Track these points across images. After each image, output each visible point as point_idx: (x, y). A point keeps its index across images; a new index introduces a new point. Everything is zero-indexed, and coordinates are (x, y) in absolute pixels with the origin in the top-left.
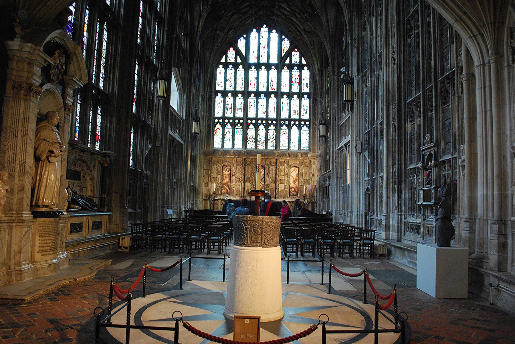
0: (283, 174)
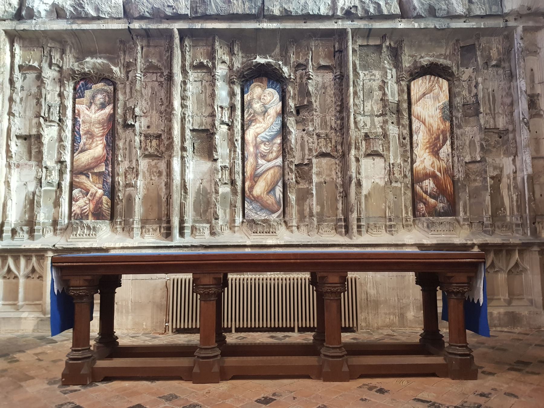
0: (377, 108)
